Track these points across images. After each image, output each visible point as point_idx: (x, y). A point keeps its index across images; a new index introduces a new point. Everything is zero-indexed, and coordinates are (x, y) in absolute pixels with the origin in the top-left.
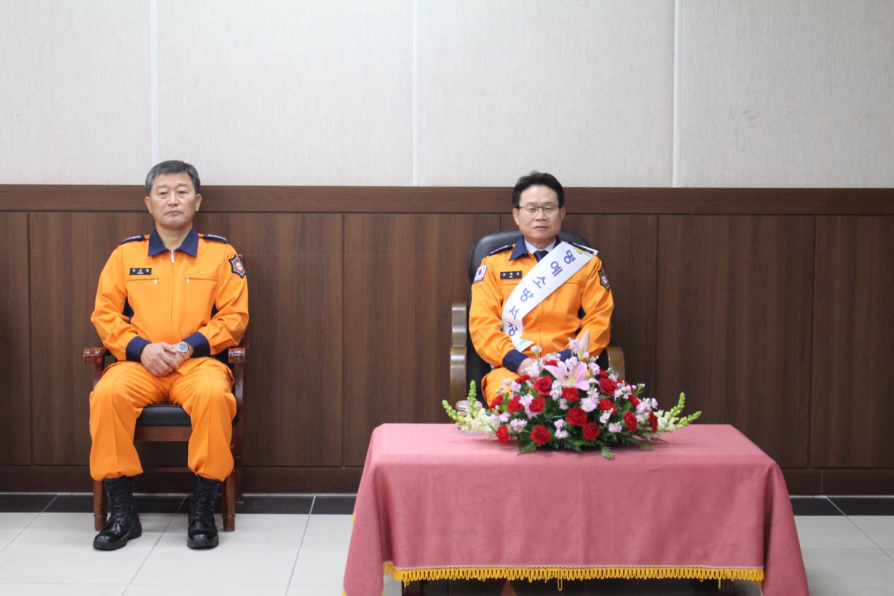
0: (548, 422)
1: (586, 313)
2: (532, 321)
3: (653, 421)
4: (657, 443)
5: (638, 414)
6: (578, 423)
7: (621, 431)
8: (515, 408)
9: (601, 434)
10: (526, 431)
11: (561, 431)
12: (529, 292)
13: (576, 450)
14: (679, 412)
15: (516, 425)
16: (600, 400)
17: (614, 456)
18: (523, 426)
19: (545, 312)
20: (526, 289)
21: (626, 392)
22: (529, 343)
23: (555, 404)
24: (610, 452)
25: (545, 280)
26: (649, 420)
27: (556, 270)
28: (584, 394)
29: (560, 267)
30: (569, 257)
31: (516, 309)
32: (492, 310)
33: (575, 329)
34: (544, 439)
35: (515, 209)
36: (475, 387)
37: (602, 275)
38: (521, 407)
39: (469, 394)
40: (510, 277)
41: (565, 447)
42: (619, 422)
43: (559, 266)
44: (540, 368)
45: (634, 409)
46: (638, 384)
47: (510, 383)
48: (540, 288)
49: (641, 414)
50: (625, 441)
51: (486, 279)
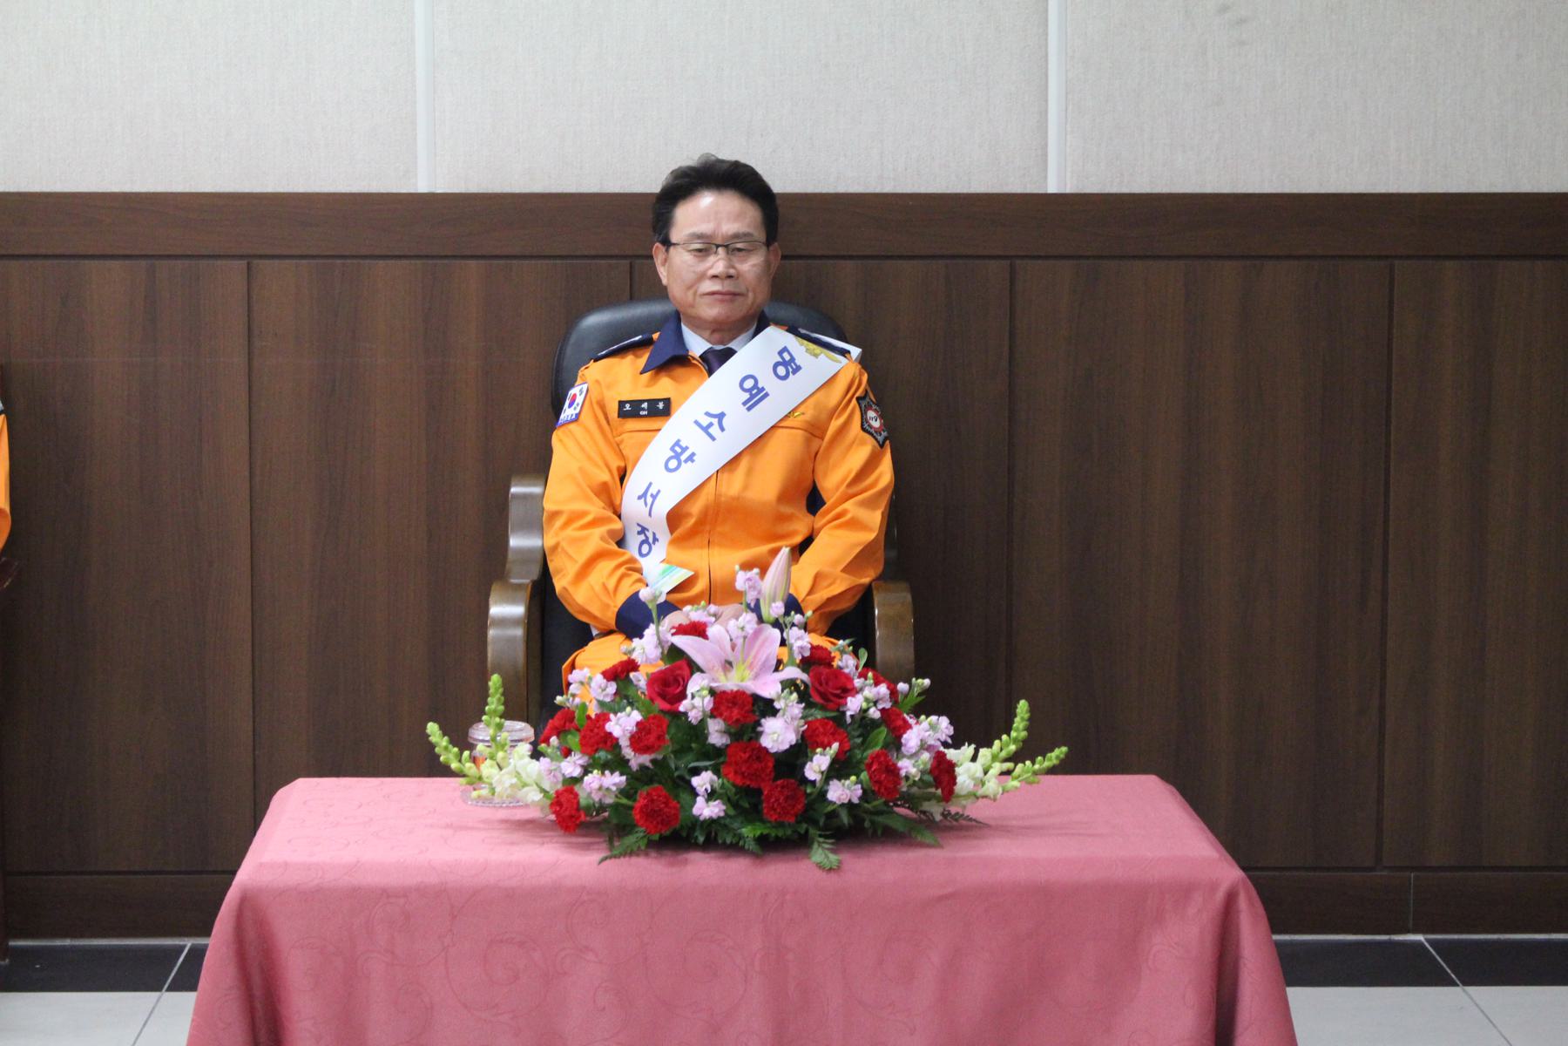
0: (681, 778)
1: (825, 499)
2: (691, 522)
3: (943, 772)
4: (959, 827)
5: (904, 756)
6: (751, 780)
7: (860, 798)
8: (598, 743)
9: (810, 807)
10: (624, 801)
11: (708, 800)
12: (685, 449)
13: (746, 847)
14: (1013, 748)
15: (595, 785)
16: (806, 723)
17: (840, 862)
18: (614, 788)
19: (723, 499)
20: (677, 443)
21: (875, 703)
22: (681, 575)
23: (698, 731)
24: (834, 851)
25: (725, 422)
26: (931, 772)
27: (752, 397)
28: (767, 708)
29: (763, 389)
30: (784, 363)
31: (653, 490)
32: (597, 494)
33: (798, 539)
34: (663, 820)
35: (658, 244)
36: (501, 690)
37: (869, 407)
38: (610, 742)
39: (487, 708)
40: (641, 413)
41: (720, 841)
42: (853, 778)
43: (760, 386)
44: (660, 643)
45: (896, 744)
46: (914, 679)
47: (590, 679)
48: (713, 439)
49: (912, 756)
50: (873, 822)
51: (586, 418)
